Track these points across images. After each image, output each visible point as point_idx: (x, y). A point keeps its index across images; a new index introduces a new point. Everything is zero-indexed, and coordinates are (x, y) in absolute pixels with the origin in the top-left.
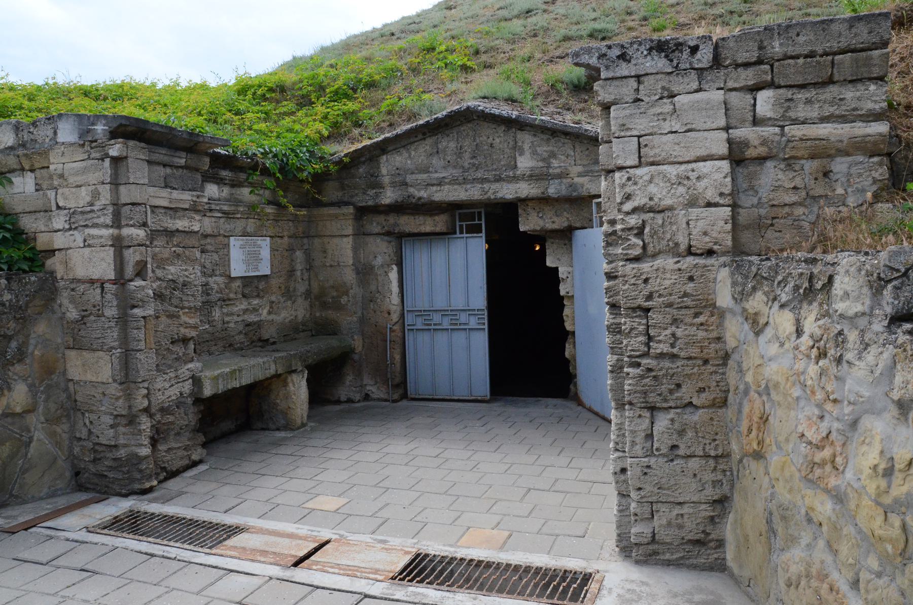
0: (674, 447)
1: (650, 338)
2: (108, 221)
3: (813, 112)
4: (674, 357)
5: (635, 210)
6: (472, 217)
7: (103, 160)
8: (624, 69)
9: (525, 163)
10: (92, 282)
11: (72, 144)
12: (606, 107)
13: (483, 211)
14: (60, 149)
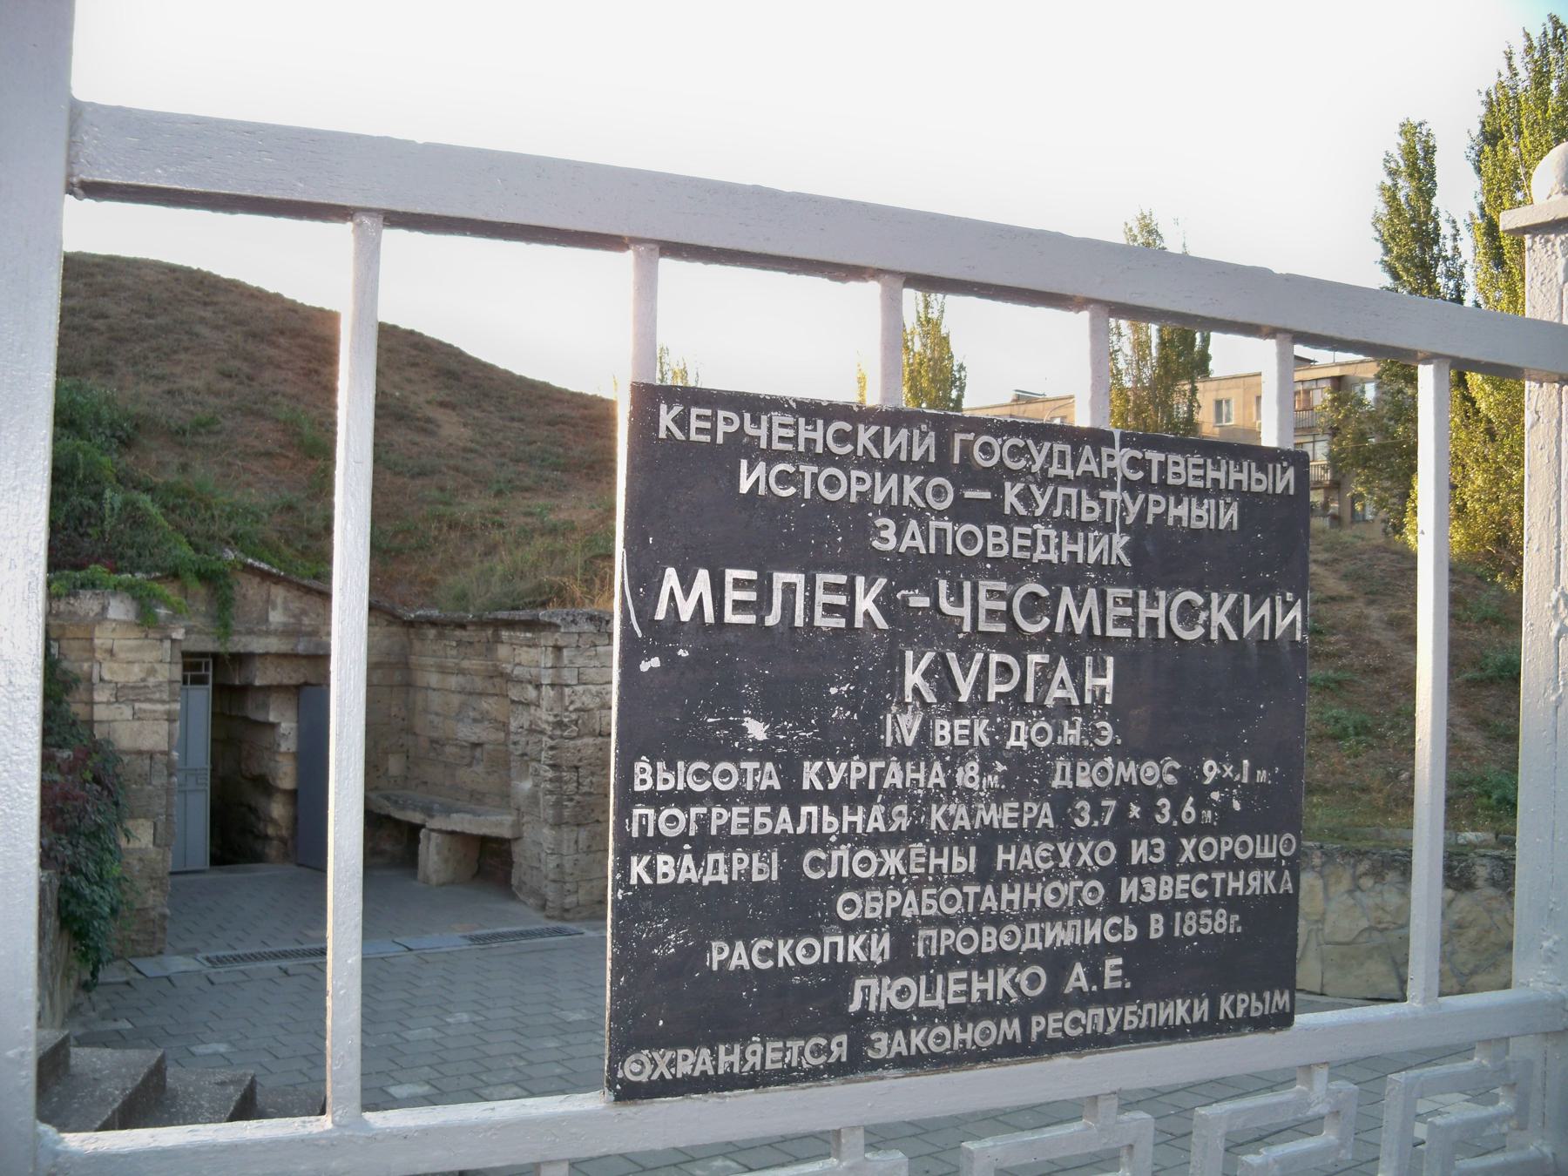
1: (579, 784)
2: (165, 697)
4: (590, 794)
5: (576, 710)
6: (197, 667)
7: (161, 640)
8: (574, 629)
9: (276, 617)
10: (140, 753)
11: (125, 622)
12: (558, 649)
13: (211, 661)
14: (109, 626)
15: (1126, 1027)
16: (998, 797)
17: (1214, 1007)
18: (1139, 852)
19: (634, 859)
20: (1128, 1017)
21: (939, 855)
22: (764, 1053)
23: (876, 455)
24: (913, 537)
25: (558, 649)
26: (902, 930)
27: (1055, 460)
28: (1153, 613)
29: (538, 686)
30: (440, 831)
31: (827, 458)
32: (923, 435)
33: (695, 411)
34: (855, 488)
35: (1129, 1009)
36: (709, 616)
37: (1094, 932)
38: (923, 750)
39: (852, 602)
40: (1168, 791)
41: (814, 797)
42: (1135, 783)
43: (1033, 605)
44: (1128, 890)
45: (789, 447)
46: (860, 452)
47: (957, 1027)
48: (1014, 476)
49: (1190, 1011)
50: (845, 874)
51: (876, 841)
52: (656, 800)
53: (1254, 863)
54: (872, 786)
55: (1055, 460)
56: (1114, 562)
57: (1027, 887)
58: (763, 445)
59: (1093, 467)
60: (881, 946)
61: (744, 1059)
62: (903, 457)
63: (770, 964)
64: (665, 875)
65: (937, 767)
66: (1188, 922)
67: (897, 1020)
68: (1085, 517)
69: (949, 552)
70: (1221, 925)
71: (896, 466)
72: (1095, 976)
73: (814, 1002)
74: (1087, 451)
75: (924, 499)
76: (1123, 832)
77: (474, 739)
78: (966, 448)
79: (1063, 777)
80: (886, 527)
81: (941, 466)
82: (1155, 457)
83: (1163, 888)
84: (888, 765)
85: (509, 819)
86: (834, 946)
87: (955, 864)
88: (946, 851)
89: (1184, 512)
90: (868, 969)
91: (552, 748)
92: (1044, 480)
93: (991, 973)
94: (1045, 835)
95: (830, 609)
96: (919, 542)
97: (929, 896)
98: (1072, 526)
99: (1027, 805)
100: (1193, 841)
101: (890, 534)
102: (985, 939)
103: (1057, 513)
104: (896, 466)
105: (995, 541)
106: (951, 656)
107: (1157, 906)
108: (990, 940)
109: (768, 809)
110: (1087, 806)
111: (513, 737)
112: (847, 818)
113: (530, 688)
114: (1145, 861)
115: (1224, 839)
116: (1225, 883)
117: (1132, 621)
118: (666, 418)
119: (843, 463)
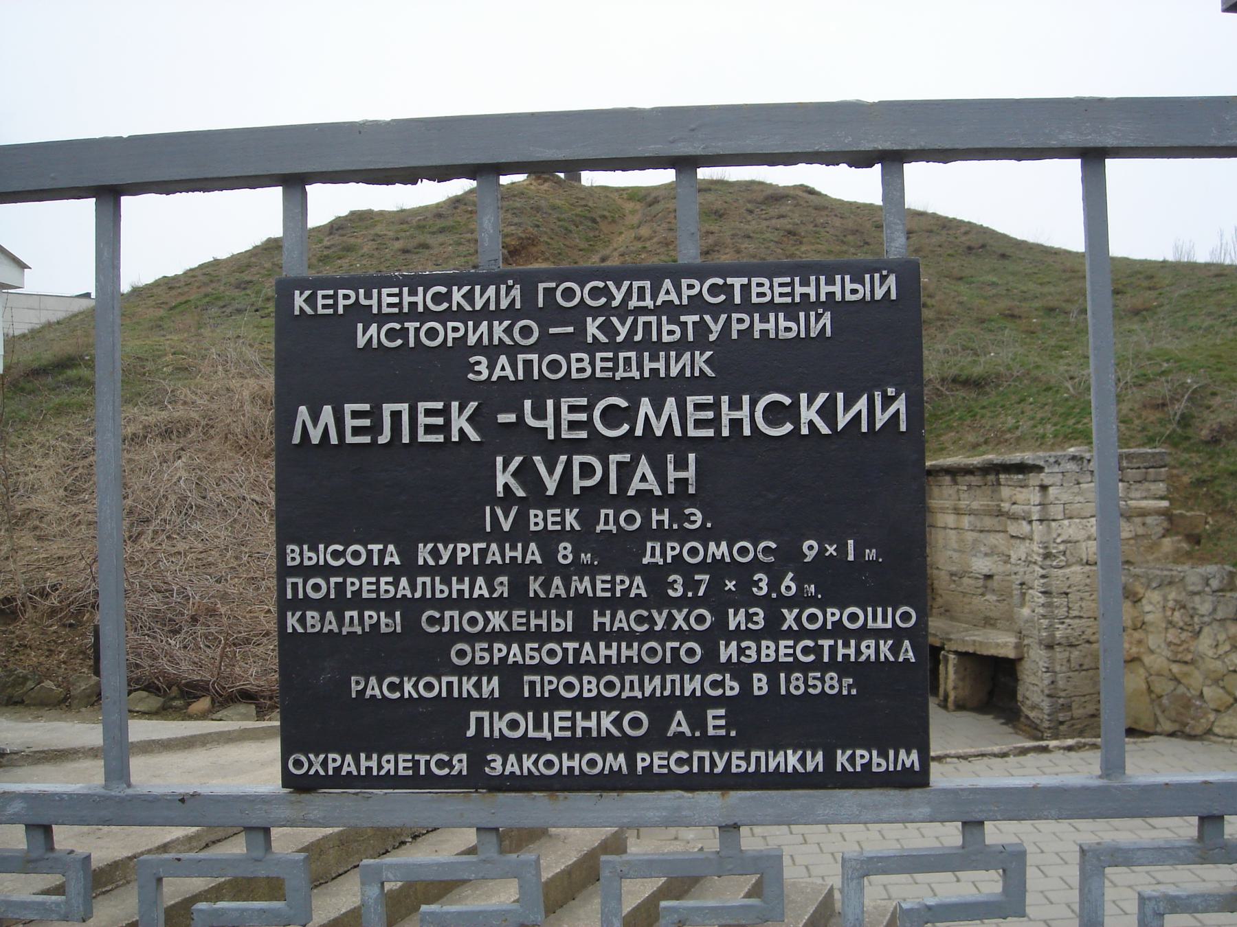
0: (1081, 665)
1: (1069, 608)
3: (1138, 495)
4: (1081, 617)
8: (1056, 469)
12: (1044, 488)
15: (734, 770)
16: (591, 571)
17: (830, 760)
18: (736, 619)
19: (289, 614)
20: (734, 762)
21: (538, 616)
22: (396, 763)
23: (468, 308)
24: (503, 369)
25: (1044, 488)
26: (510, 674)
27: (635, 296)
28: (736, 415)
29: (1030, 522)
30: (956, 652)
31: (428, 315)
32: (509, 289)
33: (320, 293)
34: (451, 335)
35: (735, 754)
36: (334, 440)
37: (692, 685)
38: (520, 533)
39: (448, 422)
40: (765, 568)
41: (426, 570)
42: (728, 560)
43: (612, 417)
44: (728, 651)
45: (396, 310)
46: (455, 308)
47: (565, 756)
48: (595, 312)
49: (802, 760)
50: (457, 629)
51: (482, 604)
52: (305, 572)
53: (863, 633)
54: (476, 562)
55: (635, 296)
56: (697, 374)
57: (624, 645)
58: (375, 311)
59: (673, 297)
60: (491, 686)
61: (380, 767)
62: (492, 307)
63: (398, 695)
64: (313, 626)
65: (533, 546)
66: (794, 683)
67: (504, 746)
68: (666, 338)
69: (536, 377)
70: (832, 687)
71: (486, 314)
72: (697, 722)
73: (440, 724)
74: (667, 284)
75: (512, 339)
76: (718, 602)
77: (986, 571)
78: (550, 293)
79: (653, 555)
80: (479, 363)
81: (529, 309)
82: (737, 282)
83: (764, 652)
84: (488, 546)
85: (1012, 640)
86: (450, 684)
87: (553, 624)
88: (545, 613)
89: (780, 327)
90: (481, 704)
91: (1043, 577)
92: (623, 311)
93: (594, 714)
94: (639, 602)
95: (429, 429)
96: (508, 372)
97: (532, 649)
98: (655, 348)
99: (618, 578)
100: (796, 611)
101: (483, 368)
102: (586, 687)
103: (638, 338)
104: (486, 314)
105: (578, 364)
106: (537, 459)
107: (758, 666)
108: (590, 687)
109: (390, 579)
110: (680, 580)
111: (1015, 569)
112: (455, 587)
113: (1024, 523)
114: (743, 627)
115: (829, 611)
116: (833, 649)
117: (715, 423)
118: (299, 301)
119: (443, 317)
